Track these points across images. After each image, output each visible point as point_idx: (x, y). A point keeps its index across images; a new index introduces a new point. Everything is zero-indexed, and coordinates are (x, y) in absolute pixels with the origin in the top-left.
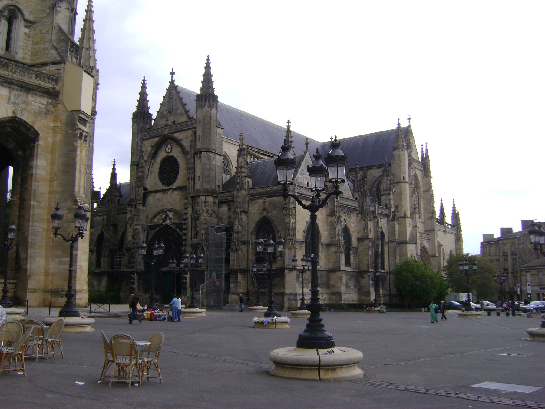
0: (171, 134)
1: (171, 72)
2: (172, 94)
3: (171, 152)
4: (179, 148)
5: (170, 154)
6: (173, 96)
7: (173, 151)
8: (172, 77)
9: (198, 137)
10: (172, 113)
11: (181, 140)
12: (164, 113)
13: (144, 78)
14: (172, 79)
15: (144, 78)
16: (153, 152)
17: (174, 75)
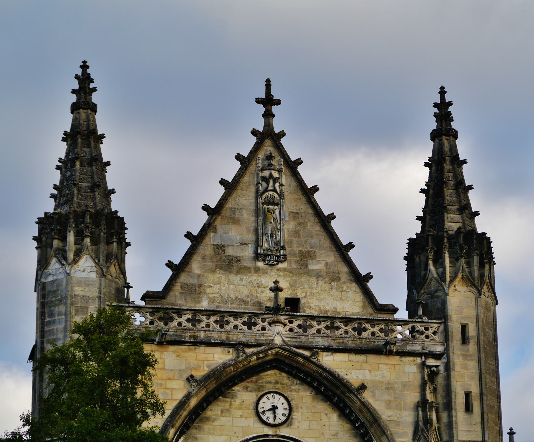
0: (307, 353)
1: (263, 95)
2: (277, 185)
3: (288, 421)
4: (334, 417)
5: (284, 431)
6: (281, 195)
7: (296, 424)
8: (268, 115)
9: (459, 400)
10: (281, 265)
11: (363, 387)
12: (230, 251)
13: (84, 66)
14: (268, 126)
15: (84, 66)
16: (193, 402)
17: (275, 109)
